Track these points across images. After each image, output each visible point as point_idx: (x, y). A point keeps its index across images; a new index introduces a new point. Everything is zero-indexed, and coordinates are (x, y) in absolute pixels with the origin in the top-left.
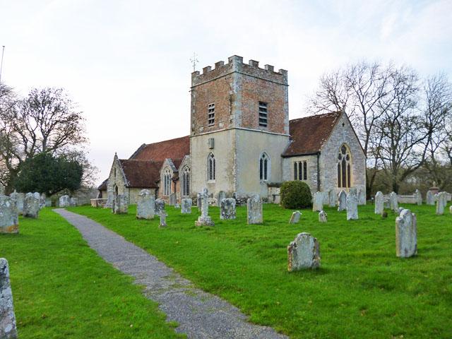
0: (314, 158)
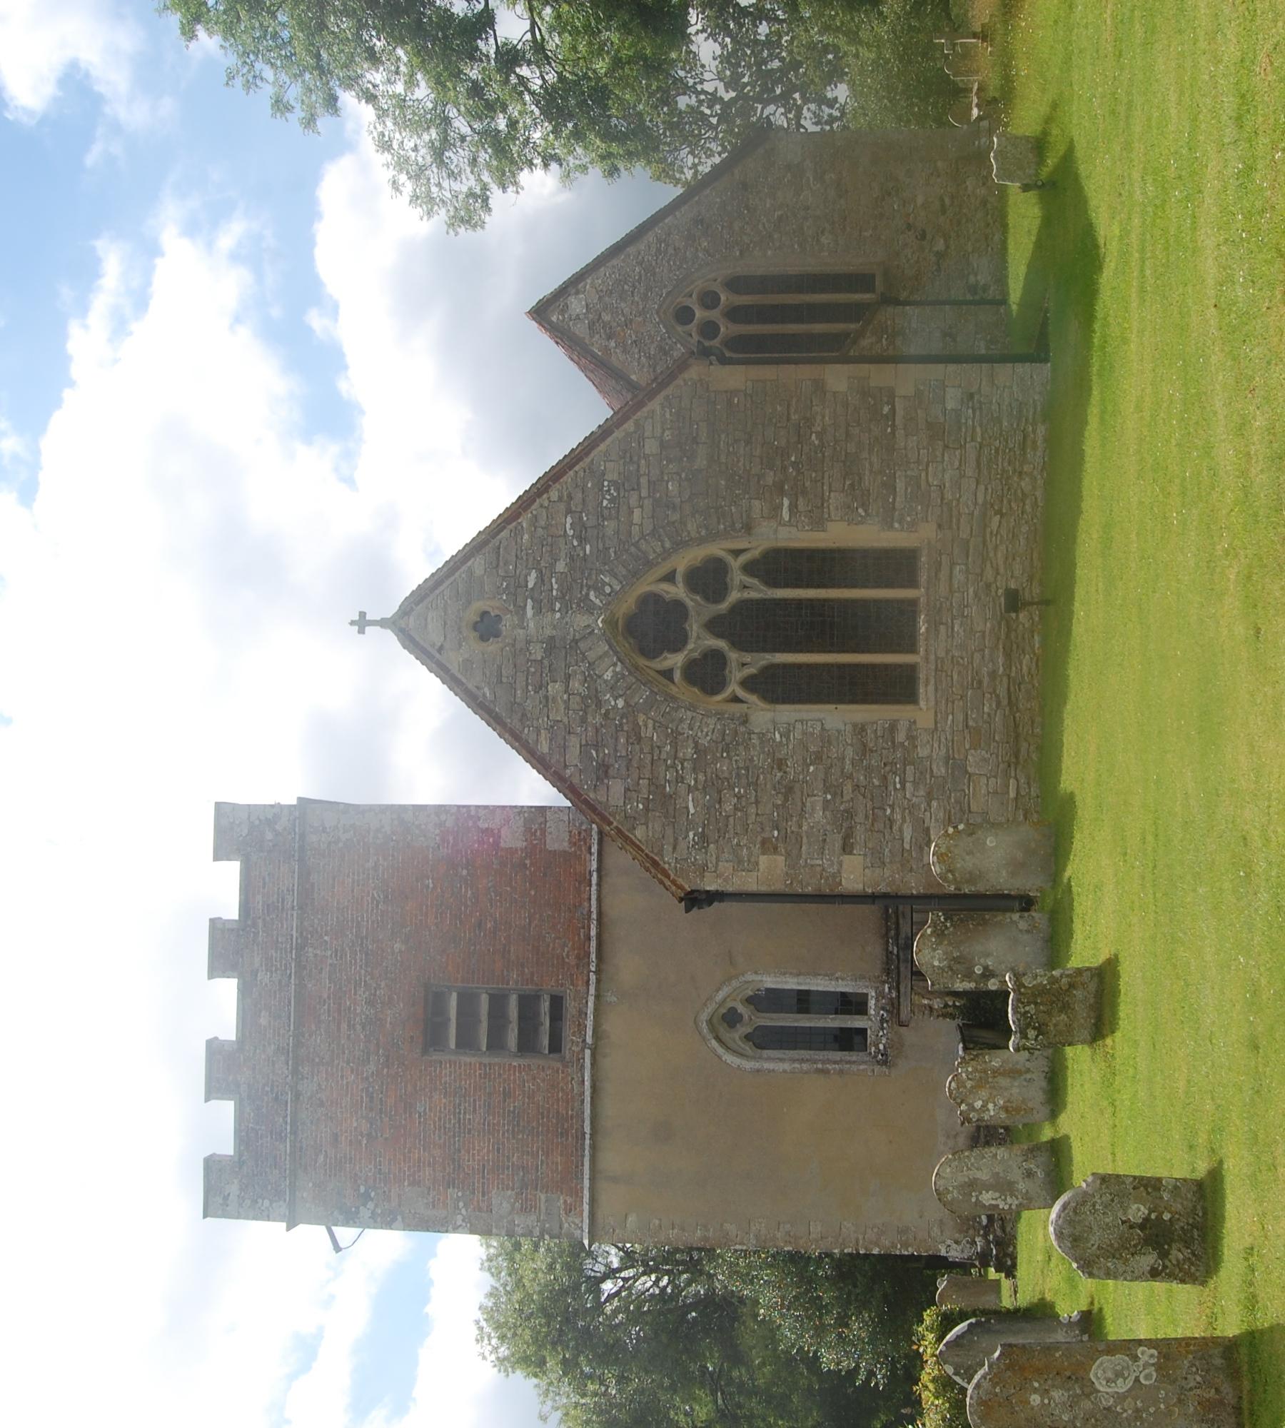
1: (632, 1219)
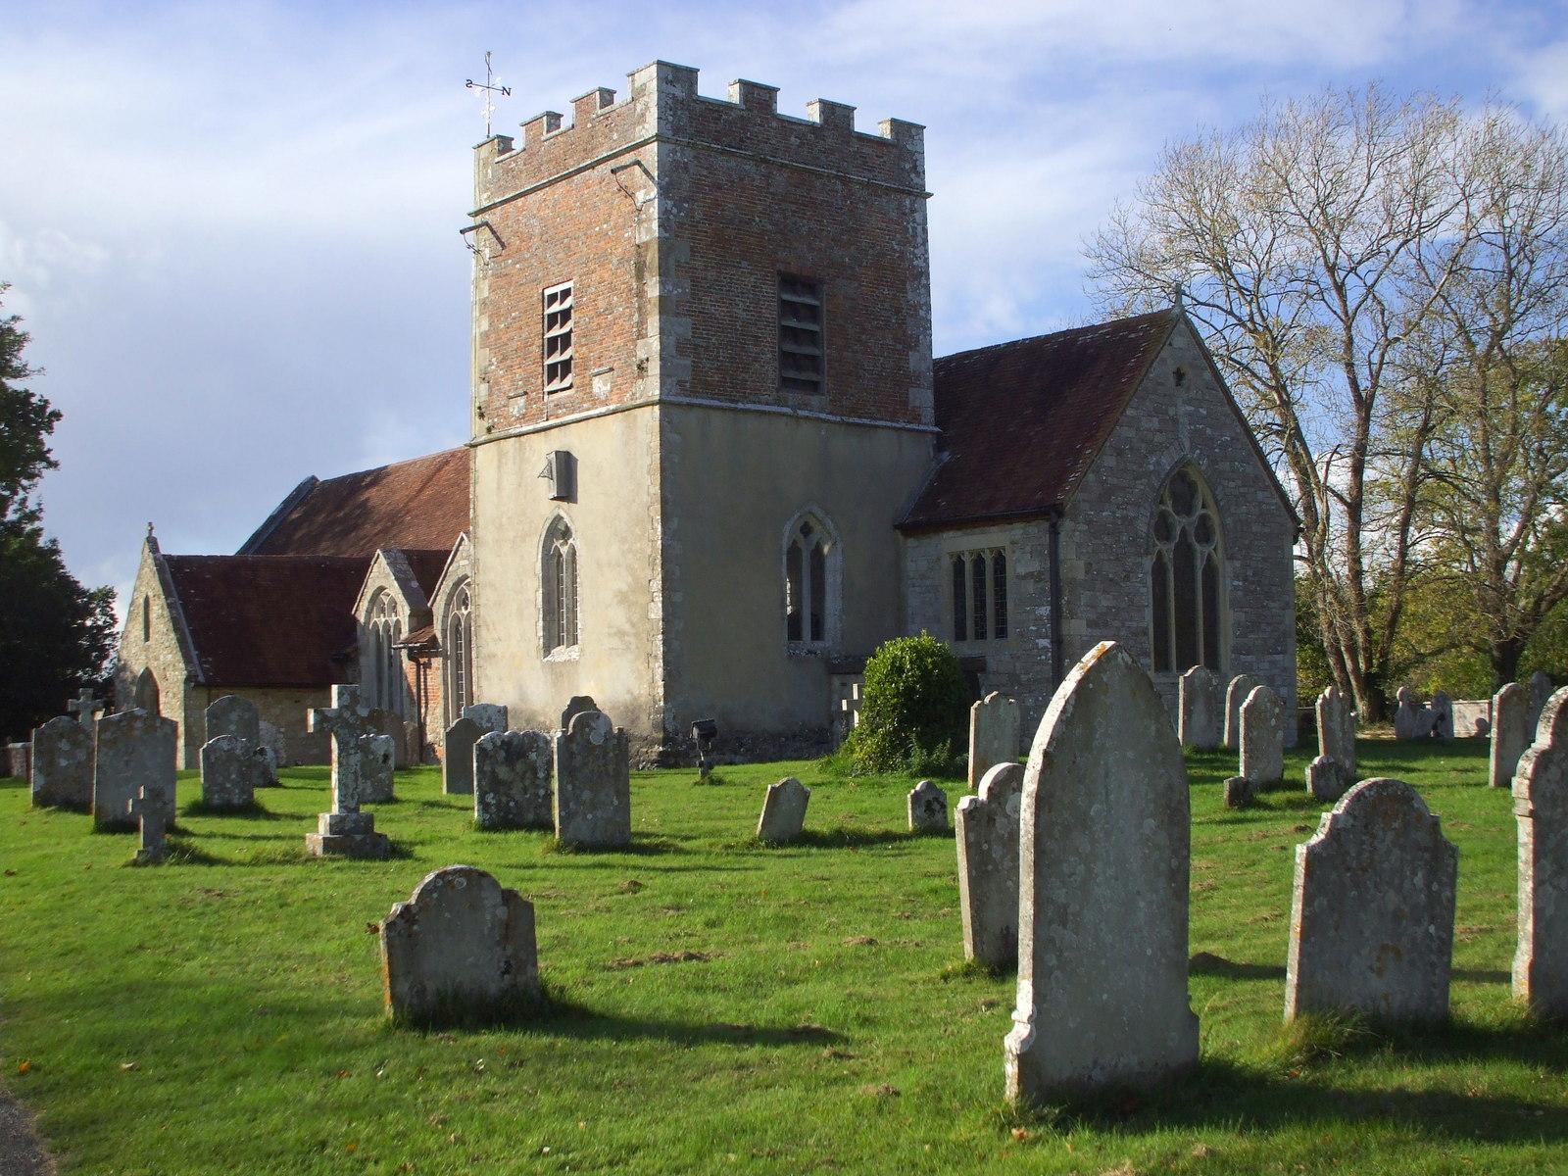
0: (1038, 530)
1: (676, 437)
